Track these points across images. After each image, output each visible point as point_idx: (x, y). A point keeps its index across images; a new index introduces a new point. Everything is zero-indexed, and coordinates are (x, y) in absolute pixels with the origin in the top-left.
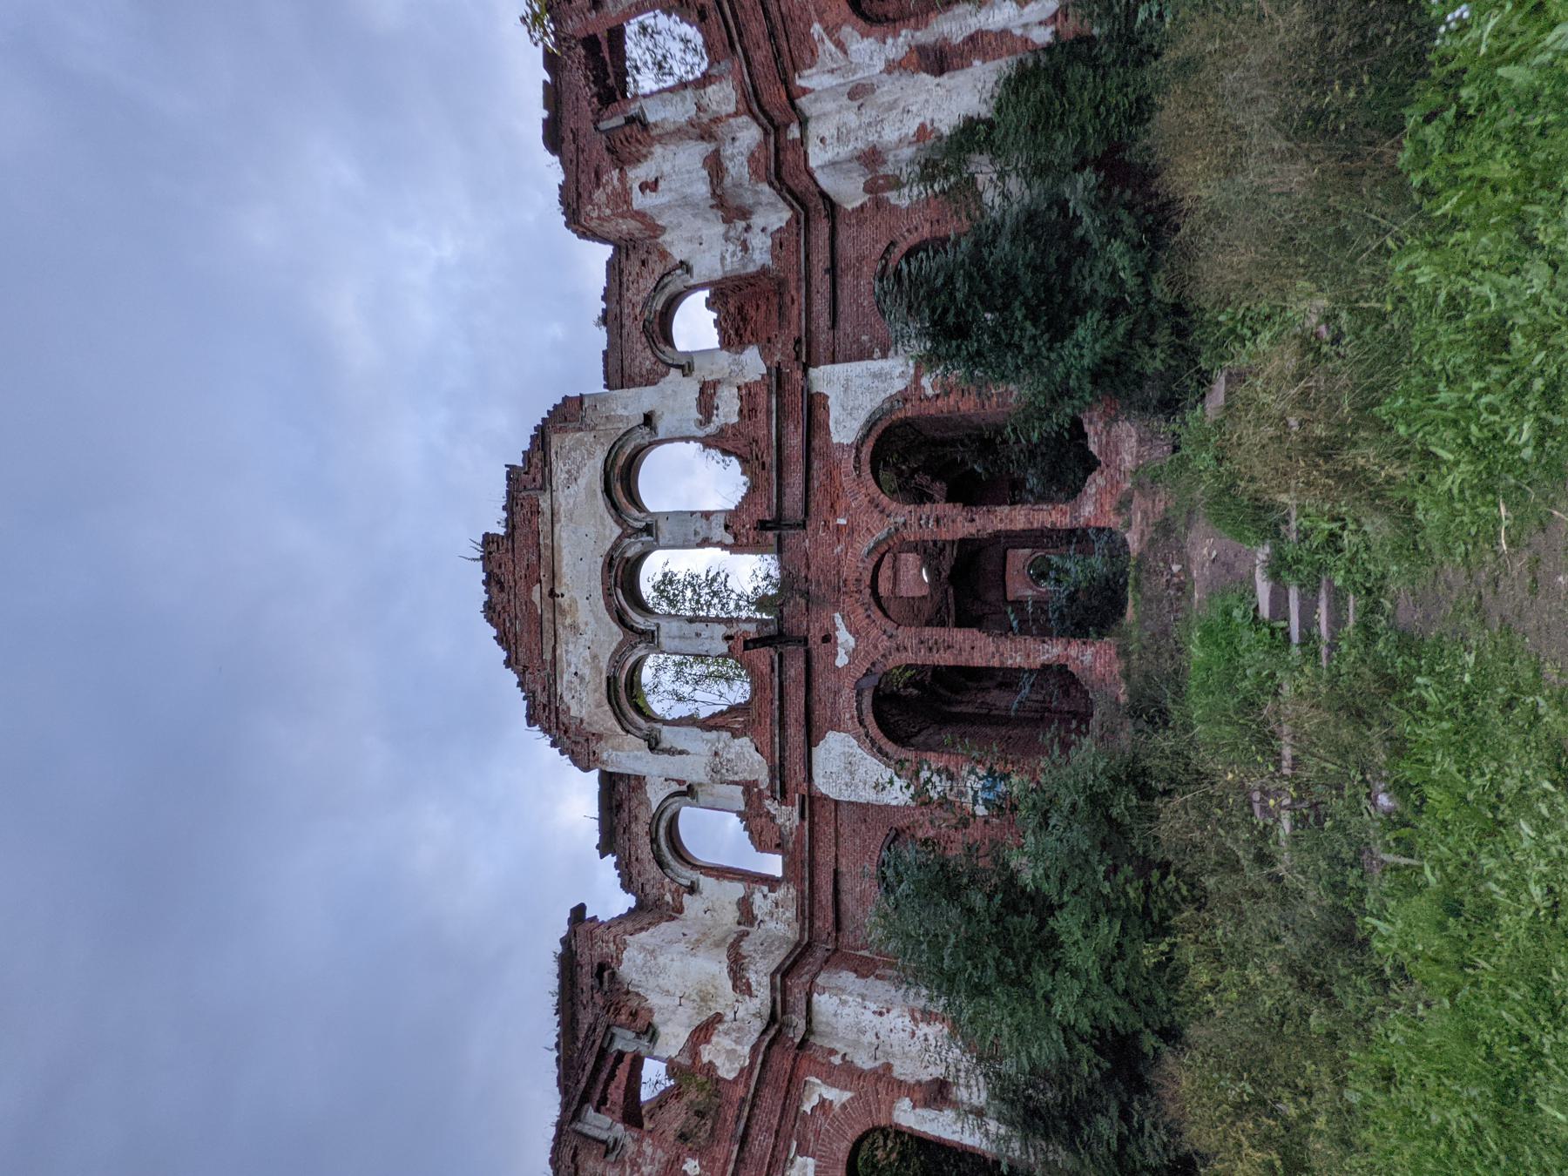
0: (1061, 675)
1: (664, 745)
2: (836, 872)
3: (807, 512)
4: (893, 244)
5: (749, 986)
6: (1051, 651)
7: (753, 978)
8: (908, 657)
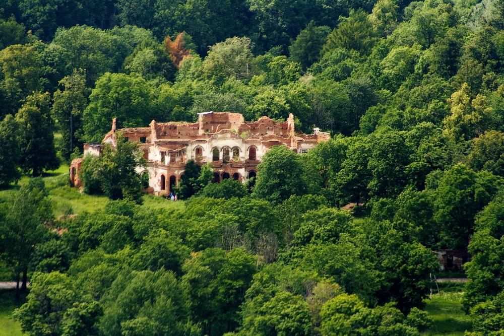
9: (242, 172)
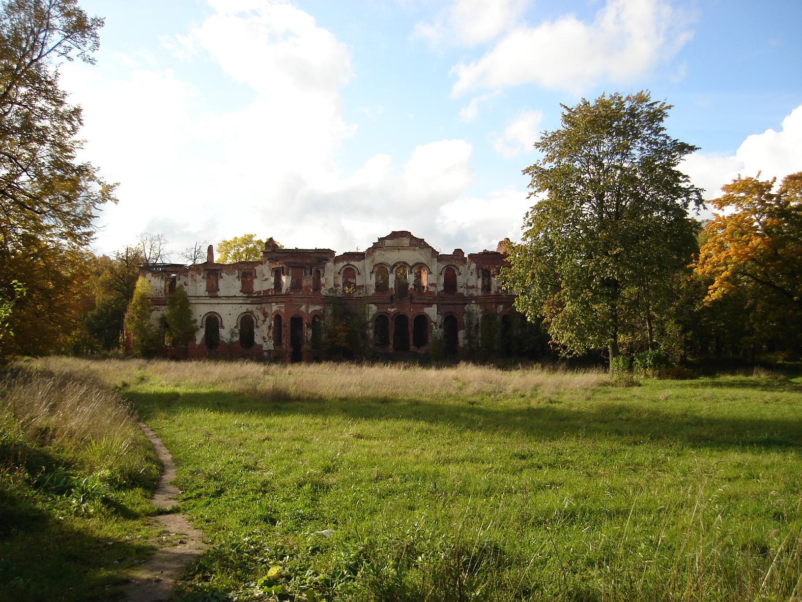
9: (432, 312)
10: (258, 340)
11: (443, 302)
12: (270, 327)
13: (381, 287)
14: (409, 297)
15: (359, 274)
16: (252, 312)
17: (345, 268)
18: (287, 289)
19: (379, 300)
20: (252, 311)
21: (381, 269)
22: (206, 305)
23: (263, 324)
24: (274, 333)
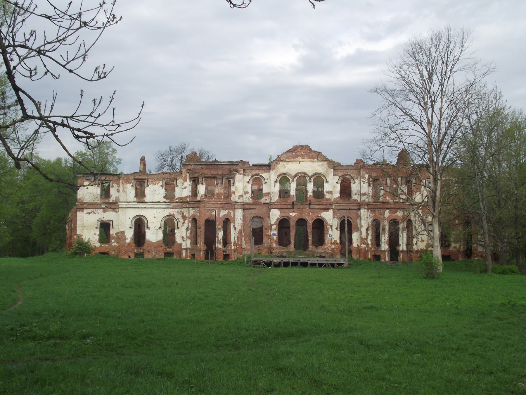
0: (289, 243)
1: (276, 183)
2: (255, 209)
3: (312, 209)
4: (352, 219)
5: (240, 198)
6: (293, 242)
7: (241, 199)
8: (291, 224)
9: (328, 216)
10: (178, 240)
11: (339, 208)
12: (187, 229)
13: (284, 194)
14: (308, 203)
15: (266, 183)
16: (173, 216)
17: (253, 178)
18: (202, 196)
19: (282, 206)
20: (174, 214)
21: (284, 179)
22: (134, 210)
23: (183, 225)
24: (191, 233)
